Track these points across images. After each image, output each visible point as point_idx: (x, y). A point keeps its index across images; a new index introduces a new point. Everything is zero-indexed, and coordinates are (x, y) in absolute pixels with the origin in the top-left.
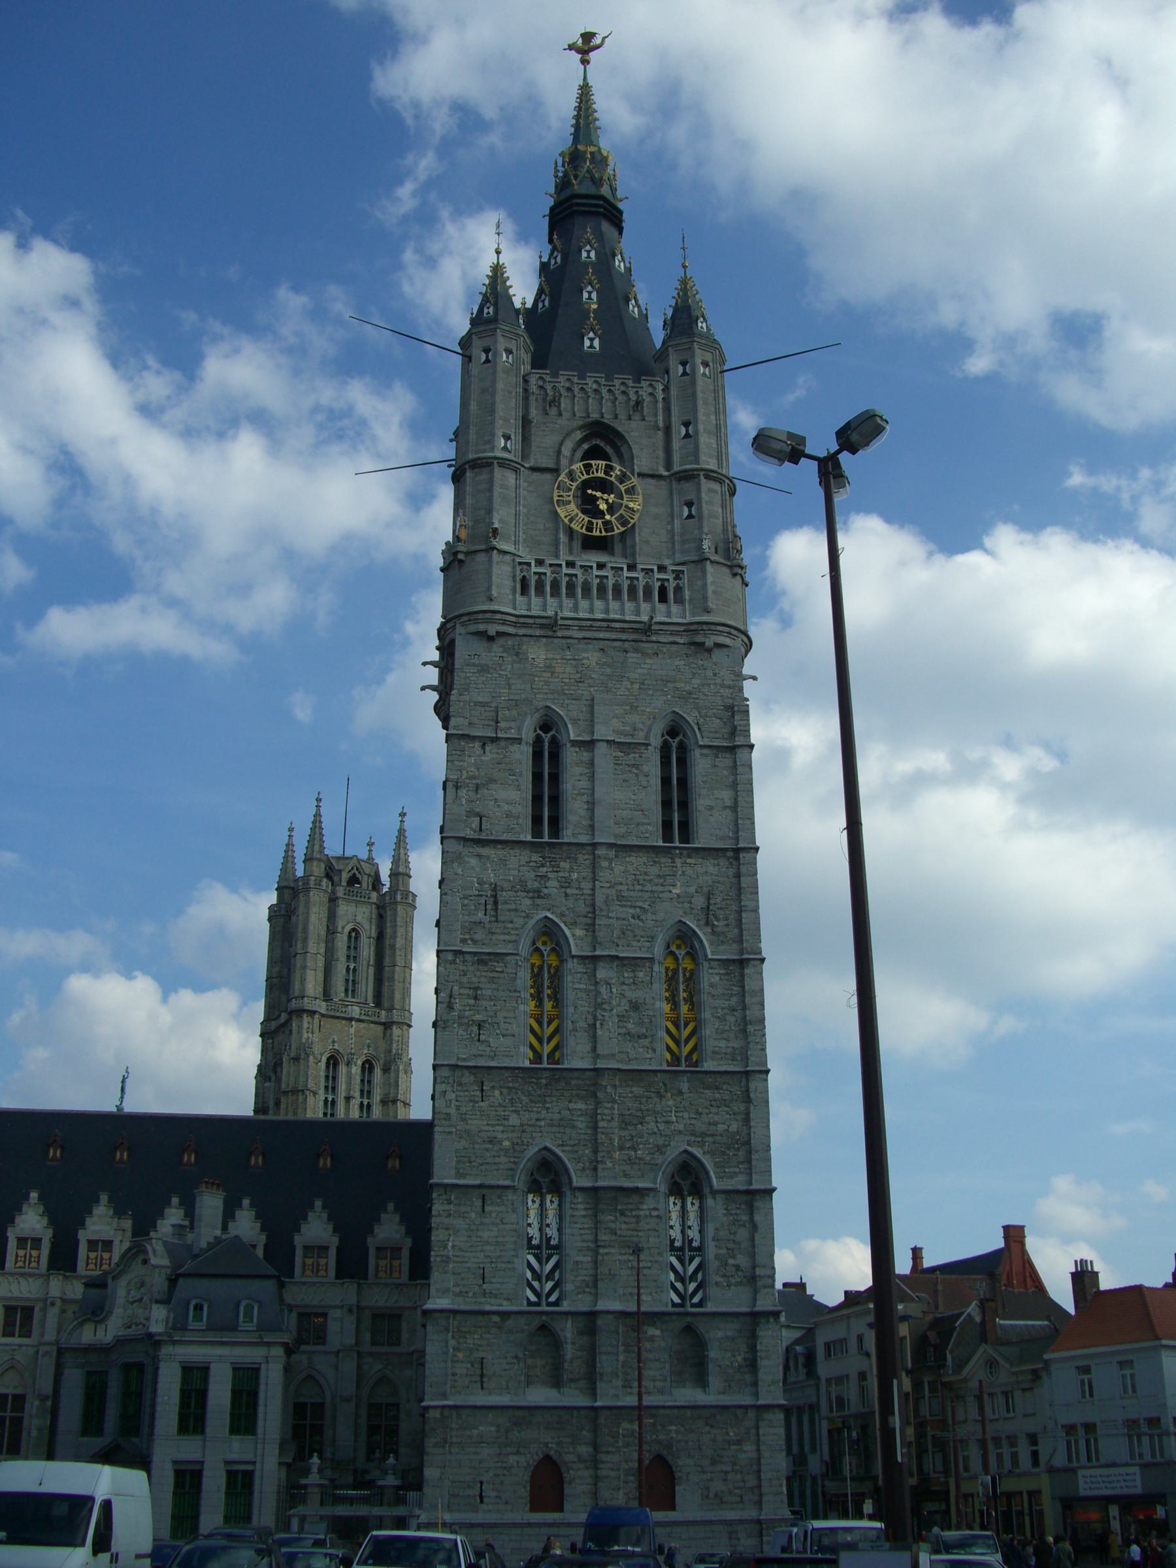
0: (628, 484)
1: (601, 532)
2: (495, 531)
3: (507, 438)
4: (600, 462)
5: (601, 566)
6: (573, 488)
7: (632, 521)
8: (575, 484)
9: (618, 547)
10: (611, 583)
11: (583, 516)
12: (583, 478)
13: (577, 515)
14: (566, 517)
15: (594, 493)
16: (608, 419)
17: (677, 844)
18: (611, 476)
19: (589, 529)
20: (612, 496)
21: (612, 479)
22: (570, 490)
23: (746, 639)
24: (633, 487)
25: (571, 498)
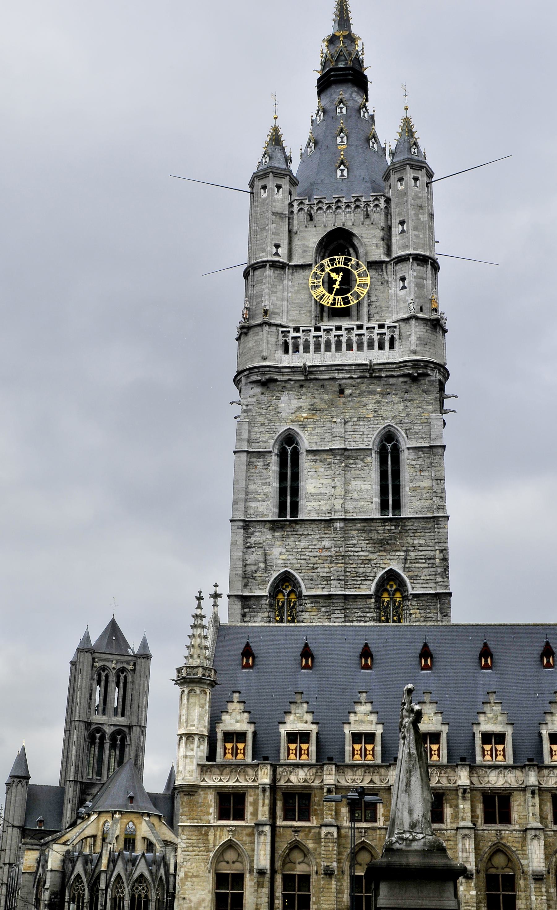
1: (341, 305)
2: (266, 312)
3: (277, 246)
4: (341, 257)
5: (339, 328)
6: (322, 276)
7: (362, 296)
9: (354, 313)
10: (344, 340)
13: (323, 295)
14: (317, 297)
16: (348, 226)
17: (391, 516)
18: (348, 266)
21: (349, 268)
23: (442, 370)
24: (363, 272)
25: (321, 284)
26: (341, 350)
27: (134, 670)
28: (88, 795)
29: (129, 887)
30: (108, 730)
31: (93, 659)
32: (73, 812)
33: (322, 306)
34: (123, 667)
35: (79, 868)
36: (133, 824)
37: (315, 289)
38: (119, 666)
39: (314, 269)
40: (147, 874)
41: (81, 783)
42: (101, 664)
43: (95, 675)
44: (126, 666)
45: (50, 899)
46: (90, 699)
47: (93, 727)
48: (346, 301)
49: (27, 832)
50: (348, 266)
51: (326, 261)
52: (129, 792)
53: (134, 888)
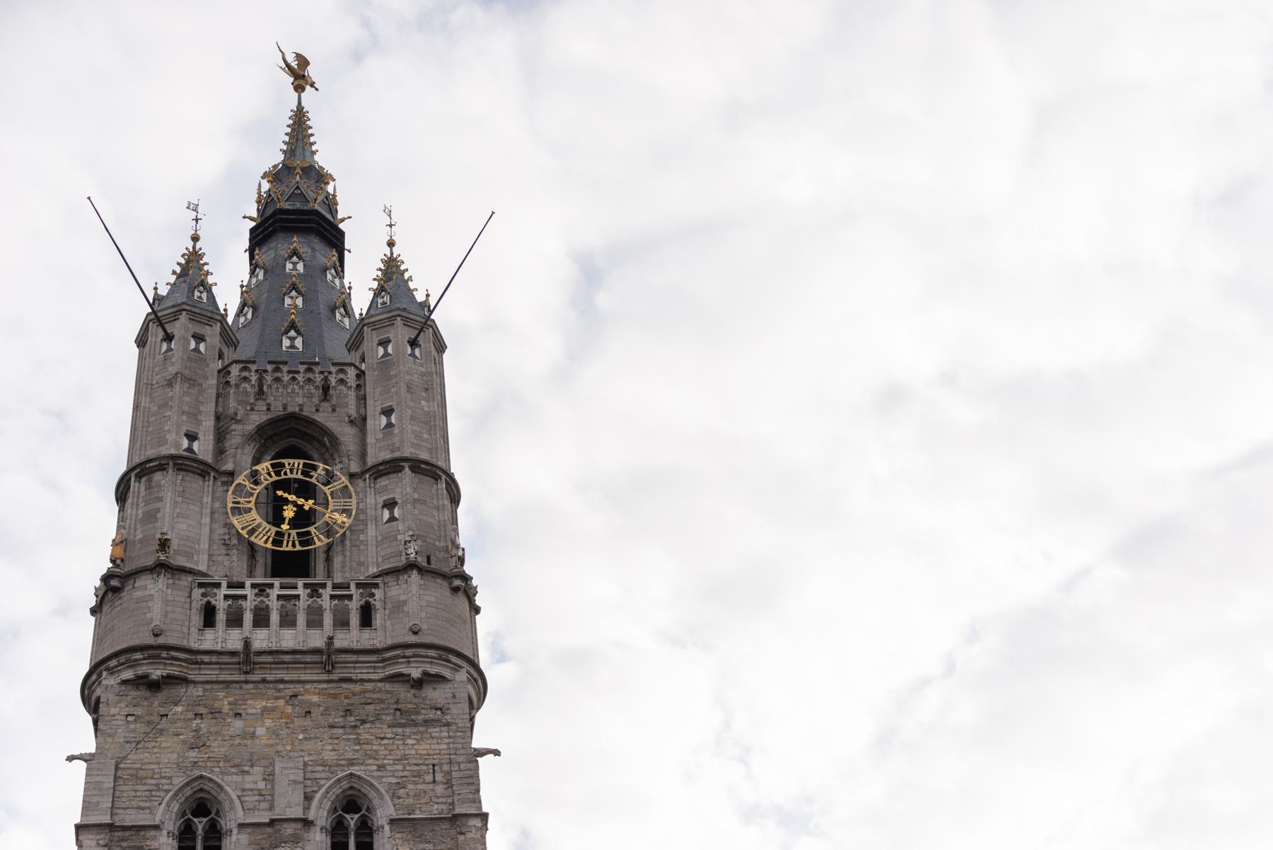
0: (336, 485)
1: (294, 545)
4: (296, 462)
7: (341, 531)
8: (259, 488)
9: (320, 567)
11: (268, 526)
12: (271, 480)
13: (259, 526)
14: (243, 529)
15: (286, 495)
18: (311, 477)
19: (277, 542)
20: (311, 502)
21: (313, 480)
22: (252, 495)
25: (252, 505)
26: (293, 624)
33: (252, 546)
37: (241, 514)
39: (240, 480)
48: (306, 539)
50: (311, 477)
51: (264, 467)
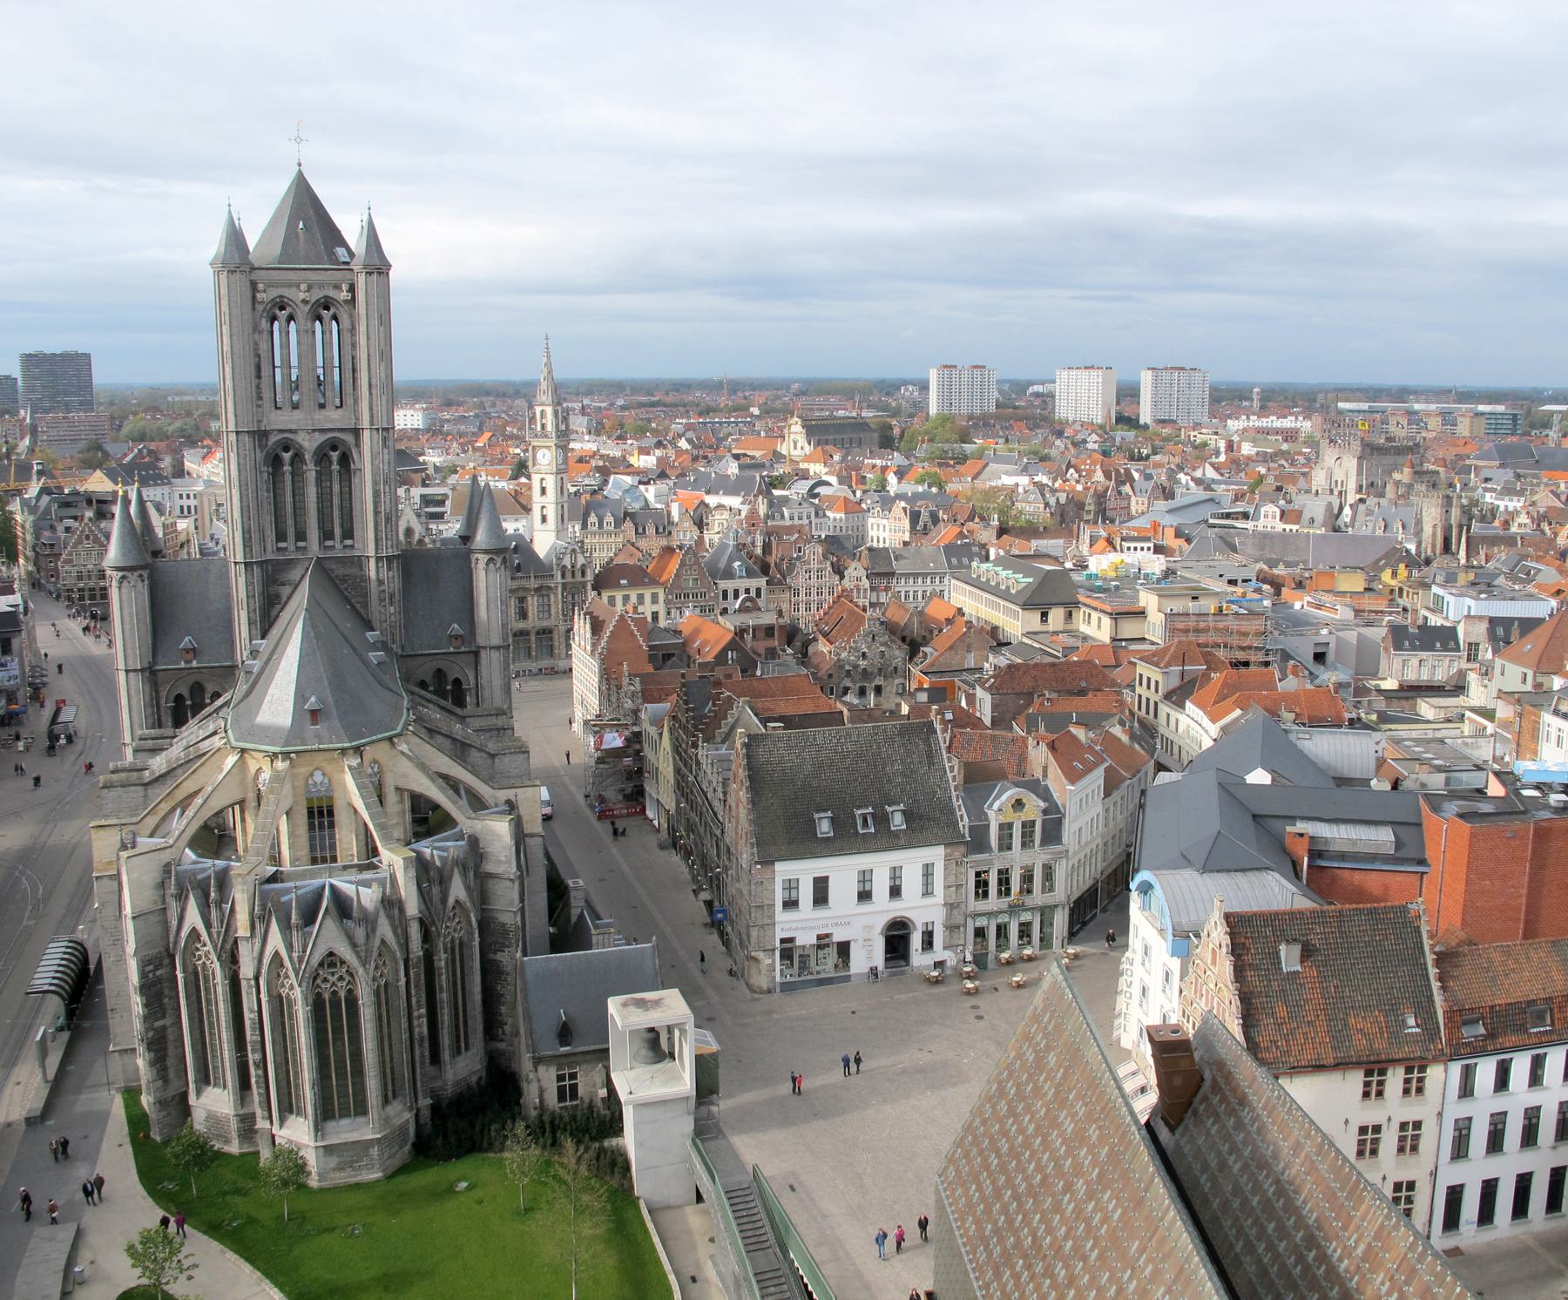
27: (352, 301)
28: (283, 584)
29: (304, 984)
30: (309, 443)
31: (254, 285)
32: (253, 627)
34: (325, 297)
35: (193, 917)
36: (324, 774)
38: (317, 295)
40: (344, 951)
41: (261, 563)
42: (273, 293)
43: (264, 321)
44: (332, 293)
45: (143, 975)
46: (259, 377)
47: (273, 439)
49: (160, 674)
52: (307, 695)
53: (318, 981)
